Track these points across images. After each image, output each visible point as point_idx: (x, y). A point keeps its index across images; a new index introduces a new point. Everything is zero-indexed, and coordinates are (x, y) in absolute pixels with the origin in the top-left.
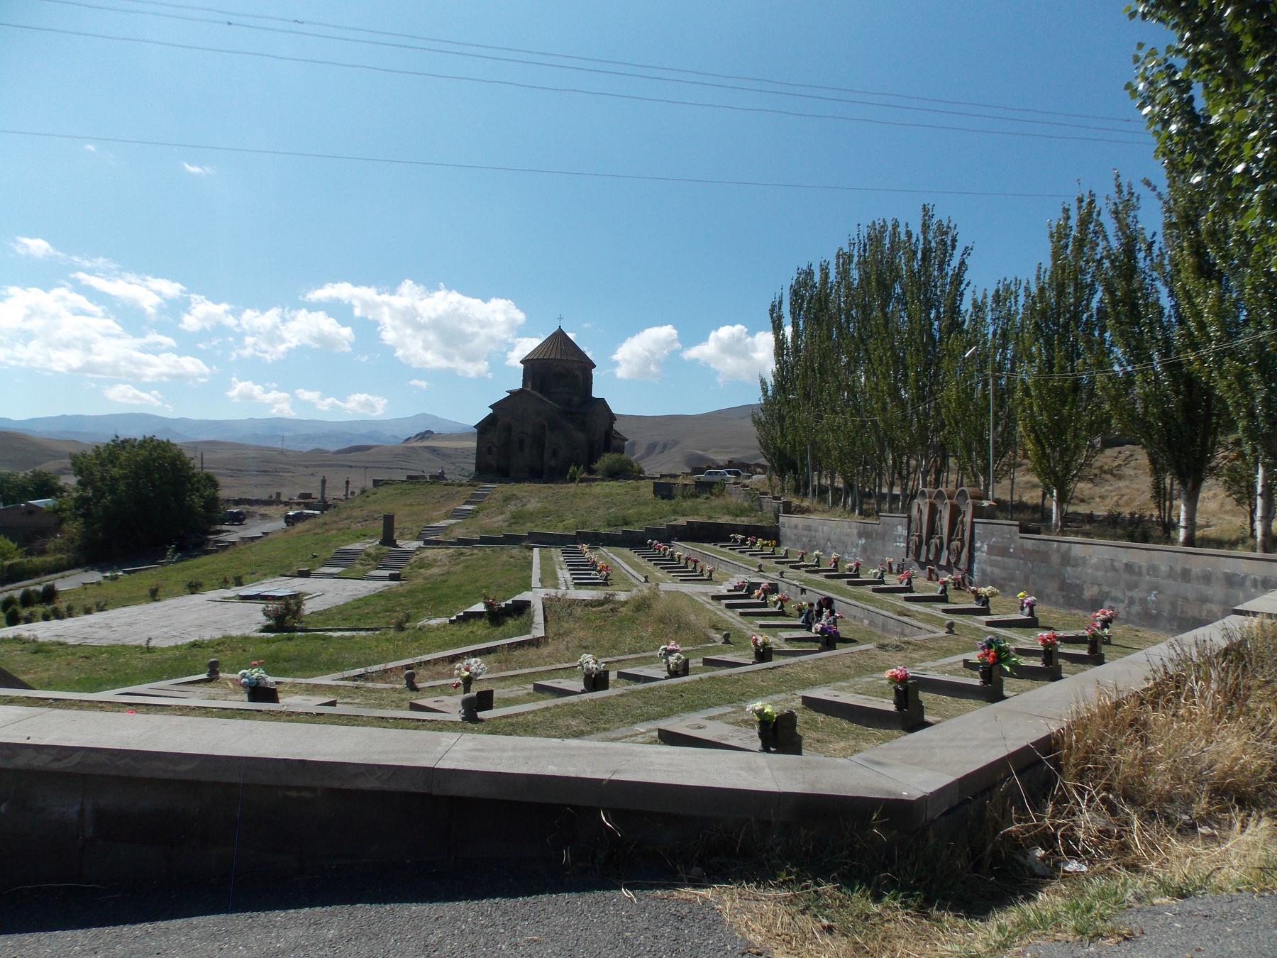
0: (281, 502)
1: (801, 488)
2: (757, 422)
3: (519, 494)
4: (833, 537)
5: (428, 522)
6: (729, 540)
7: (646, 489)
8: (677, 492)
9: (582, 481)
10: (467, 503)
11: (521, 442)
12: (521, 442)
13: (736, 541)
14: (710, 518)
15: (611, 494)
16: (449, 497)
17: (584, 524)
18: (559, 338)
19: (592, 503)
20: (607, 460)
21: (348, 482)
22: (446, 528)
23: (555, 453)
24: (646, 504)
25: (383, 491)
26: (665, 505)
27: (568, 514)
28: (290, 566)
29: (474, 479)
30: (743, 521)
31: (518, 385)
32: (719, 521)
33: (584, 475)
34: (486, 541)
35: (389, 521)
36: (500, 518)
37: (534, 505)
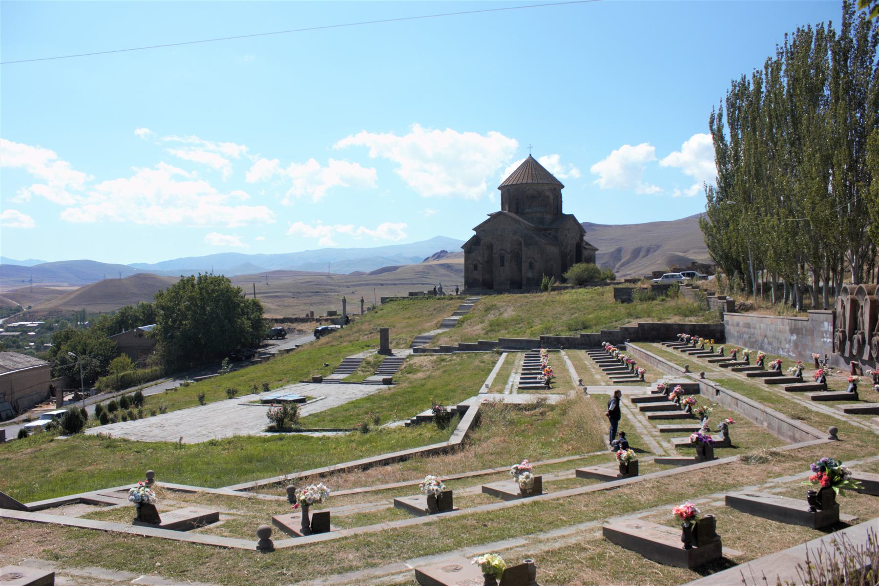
0: (313, 320)
1: (748, 288)
2: (705, 227)
3: (499, 304)
4: (769, 334)
5: (420, 332)
6: (677, 339)
7: (608, 292)
8: (636, 296)
9: (554, 289)
10: (455, 314)
11: (502, 258)
12: (502, 258)
13: (682, 340)
14: (660, 319)
15: (577, 300)
16: (440, 310)
17: (548, 329)
18: (531, 165)
19: (559, 310)
20: (576, 269)
21: (362, 301)
22: (434, 337)
23: (531, 266)
24: (606, 308)
25: (388, 307)
26: (622, 308)
27: (537, 321)
28: (308, 373)
29: (464, 292)
30: (692, 320)
31: (498, 208)
32: (669, 322)
33: (557, 284)
34: (464, 348)
35: (384, 333)
36: (480, 326)
37: (509, 313)
